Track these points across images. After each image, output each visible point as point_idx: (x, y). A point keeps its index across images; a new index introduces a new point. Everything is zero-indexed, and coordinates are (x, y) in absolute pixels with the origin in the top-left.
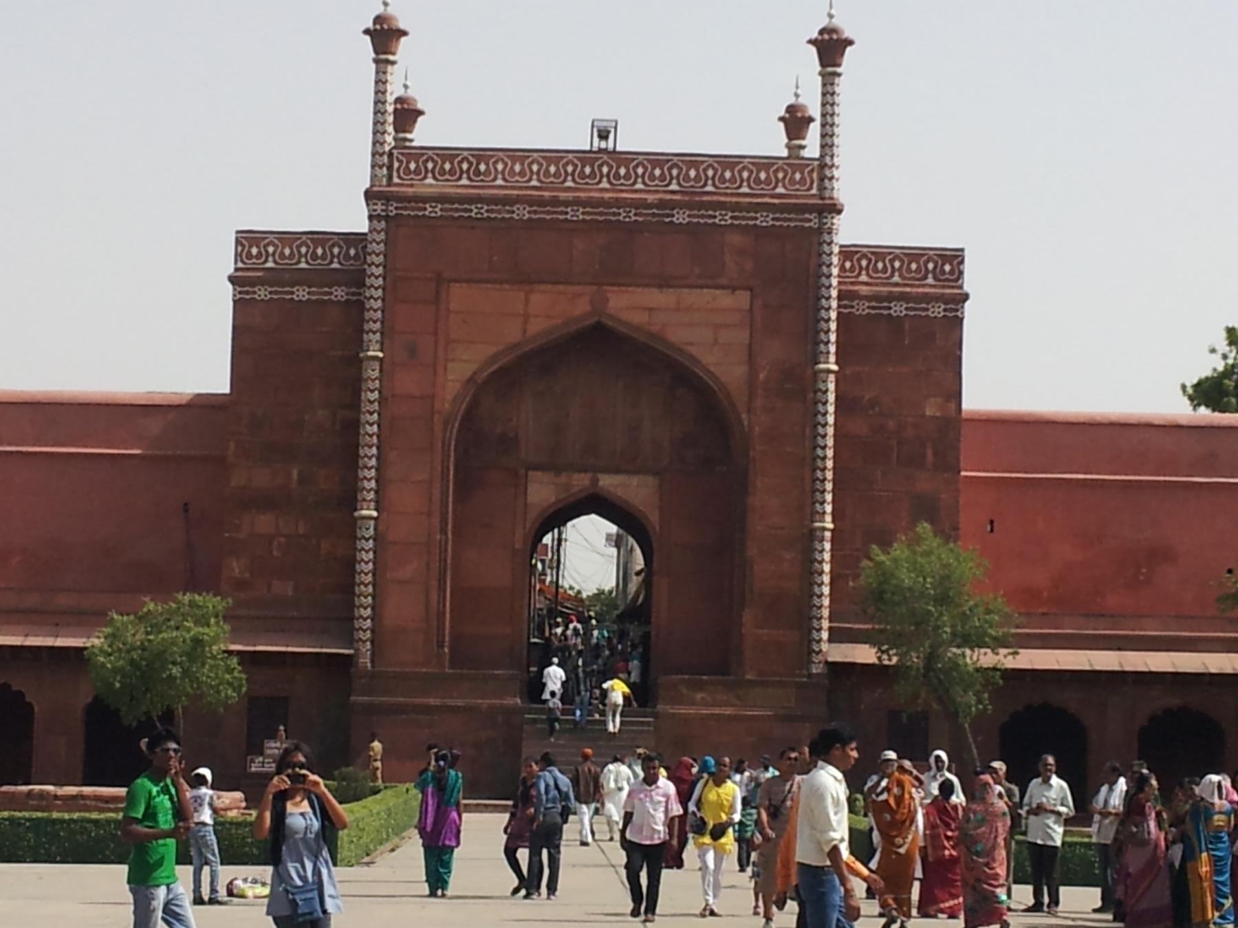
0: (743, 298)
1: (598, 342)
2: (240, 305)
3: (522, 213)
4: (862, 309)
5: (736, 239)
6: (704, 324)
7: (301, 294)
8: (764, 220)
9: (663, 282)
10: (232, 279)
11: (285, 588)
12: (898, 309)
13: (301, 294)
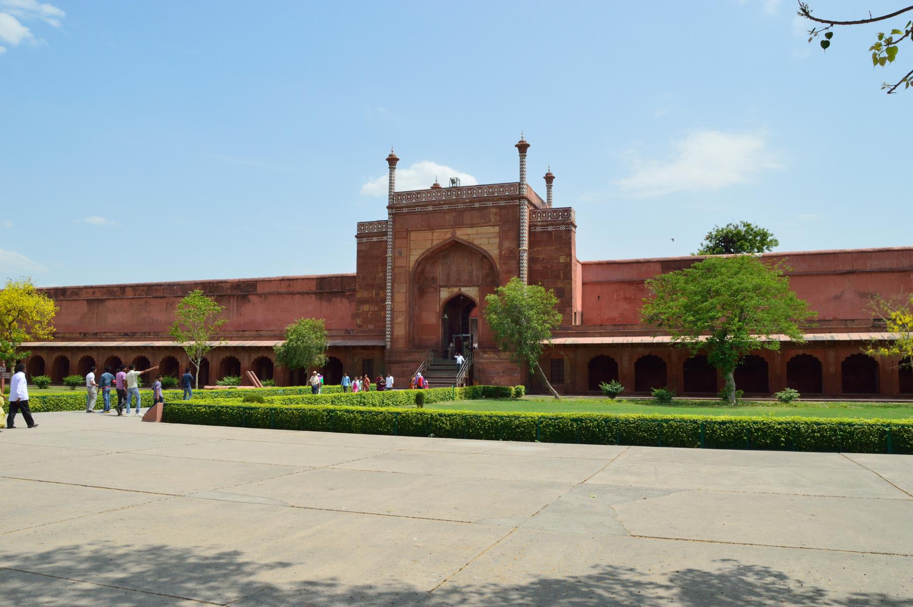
0: (497, 229)
1: (455, 246)
2: (358, 244)
3: (430, 208)
4: (539, 229)
5: (494, 210)
6: (486, 238)
7: (375, 239)
8: (502, 203)
9: (472, 226)
10: (356, 237)
11: (371, 327)
12: (550, 228)
13: (375, 239)
